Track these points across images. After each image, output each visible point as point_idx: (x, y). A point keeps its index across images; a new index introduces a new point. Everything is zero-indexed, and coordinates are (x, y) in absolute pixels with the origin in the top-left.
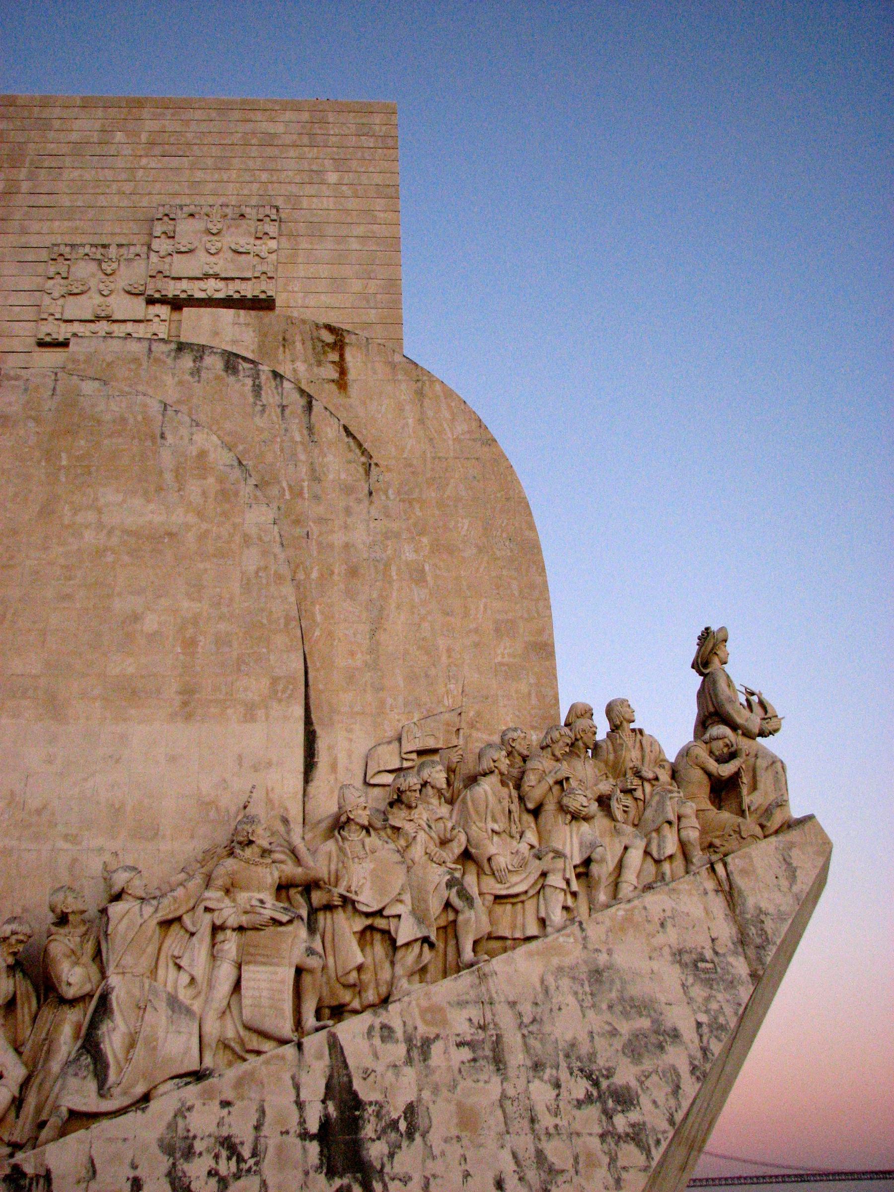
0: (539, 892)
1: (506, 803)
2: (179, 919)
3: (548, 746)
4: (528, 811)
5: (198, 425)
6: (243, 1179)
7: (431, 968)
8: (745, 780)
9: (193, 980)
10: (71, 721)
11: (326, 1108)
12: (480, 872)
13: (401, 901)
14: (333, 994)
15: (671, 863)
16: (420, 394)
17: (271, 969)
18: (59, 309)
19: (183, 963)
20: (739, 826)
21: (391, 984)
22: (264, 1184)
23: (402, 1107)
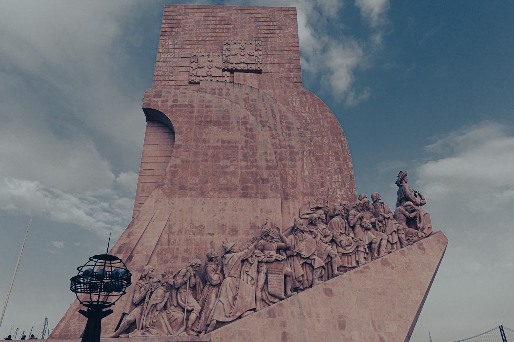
0: (356, 253)
1: (344, 224)
2: (247, 259)
3: (355, 207)
4: (350, 227)
7: (324, 276)
8: (418, 219)
9: (252, 278)
12: (337, 245)
13: (314, 254)
14: (294, 284)
15: (396, 245)
17: (277, 275)
18: (195, 72)
20: (417, 233)
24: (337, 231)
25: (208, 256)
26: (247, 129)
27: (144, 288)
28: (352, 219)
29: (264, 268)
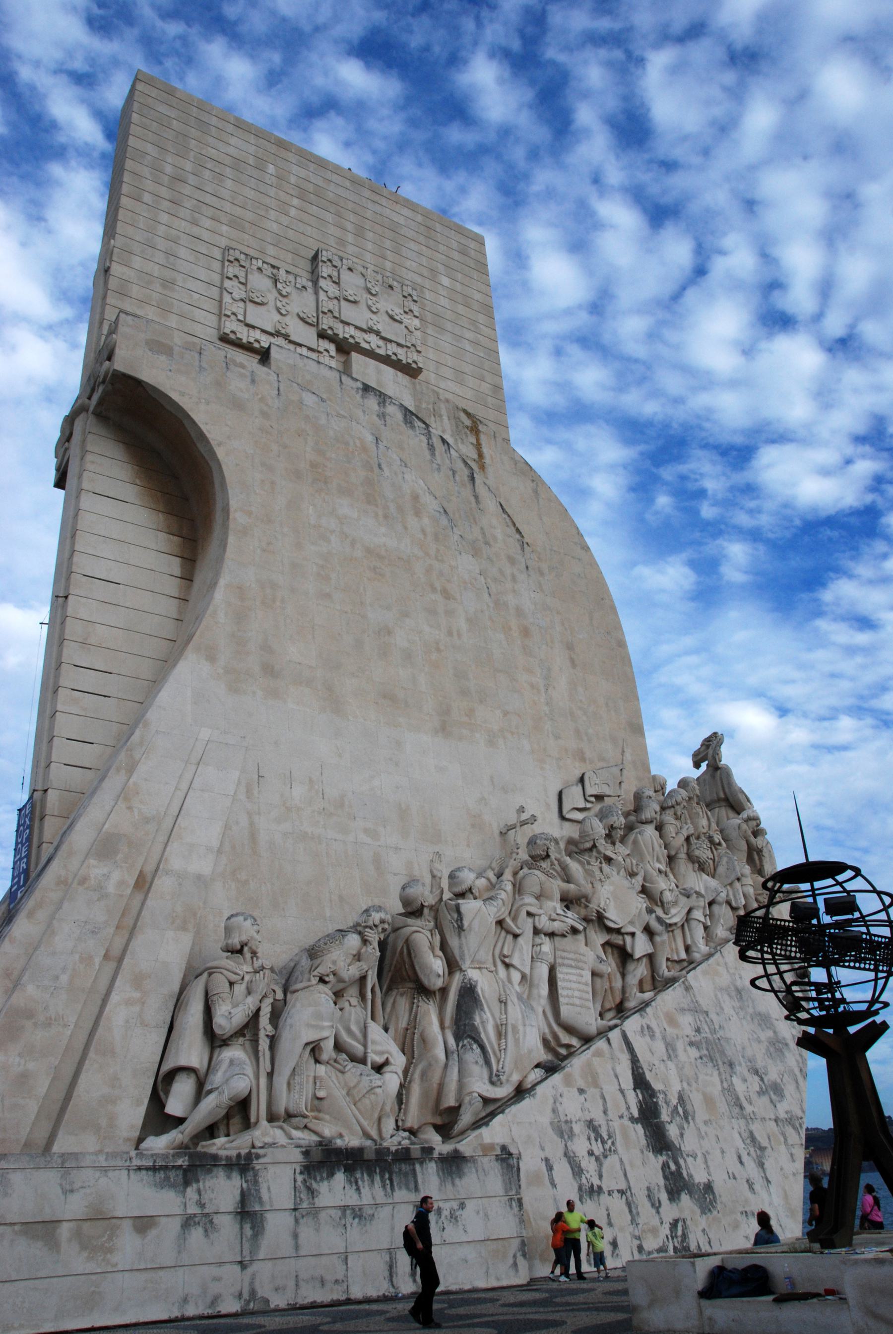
0: (683, 925)
3: (673, 807)
5: (406, 466)
6: (609, 1157)
9: (524, 977)
10: (351, 718)
11: (637, 1095)
16: (536, 492)
17: (578, 971)
18: (241, 311)
19: (515, 961)
21: (624, 990)
22: (621, 1160)
23: (676, 1096)
24: (652, 864)
25: (406, 902)
26: (423, 531)
27: (244, 986)
28: (674, 838)
29: (547, 946)
